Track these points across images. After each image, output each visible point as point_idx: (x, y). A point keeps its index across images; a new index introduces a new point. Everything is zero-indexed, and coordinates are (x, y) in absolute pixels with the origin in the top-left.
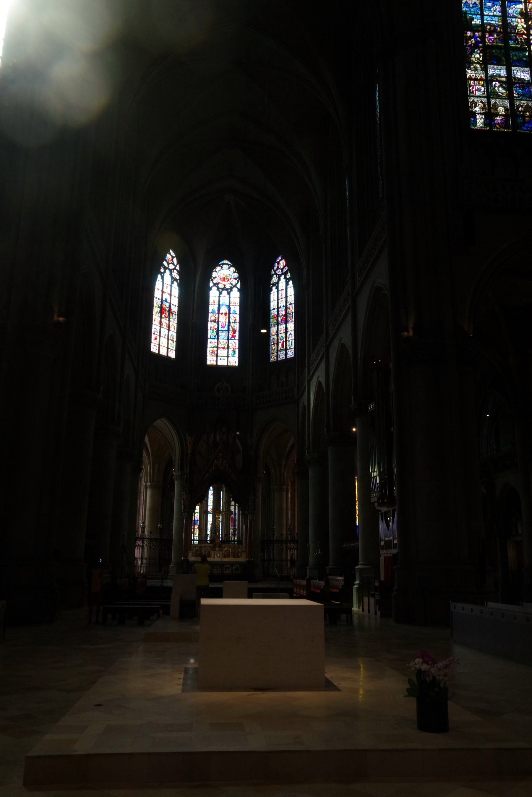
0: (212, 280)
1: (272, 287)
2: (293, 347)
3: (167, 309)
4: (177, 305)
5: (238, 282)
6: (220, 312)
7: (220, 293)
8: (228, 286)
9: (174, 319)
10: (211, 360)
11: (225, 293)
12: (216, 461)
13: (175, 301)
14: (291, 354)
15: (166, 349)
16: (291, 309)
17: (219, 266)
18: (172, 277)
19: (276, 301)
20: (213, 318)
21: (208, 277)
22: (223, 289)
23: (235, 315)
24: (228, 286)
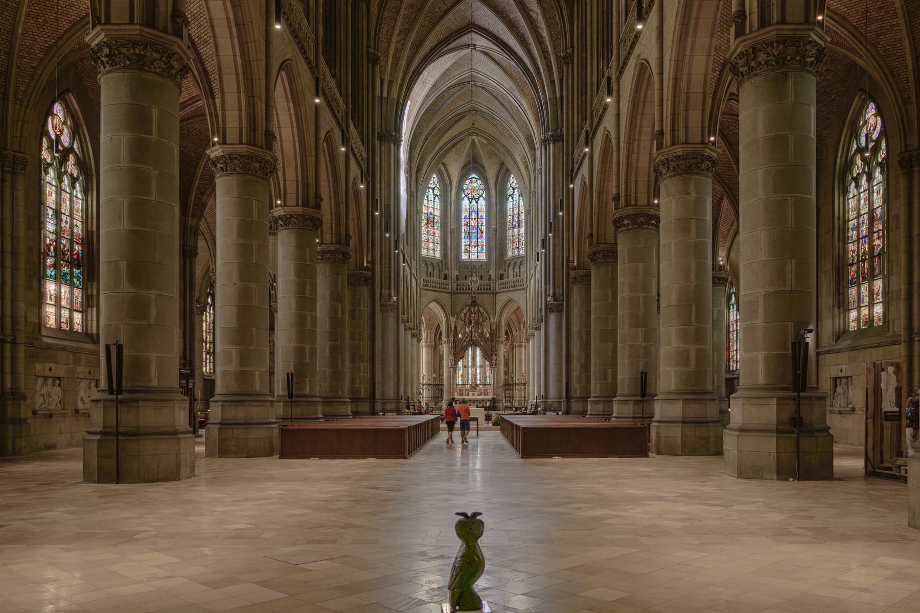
9: (437, 226)
10: (464, 257)
11: (474, 202)
13: (437, 213)
14: (522, 252)
16: (523, 217)
21: (460, 189)
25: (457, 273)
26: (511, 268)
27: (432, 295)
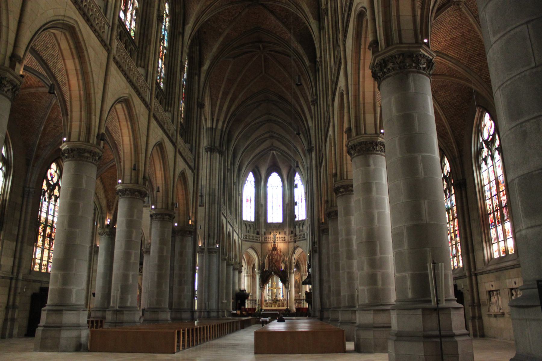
25: (264, 230)
27: (249, 244)
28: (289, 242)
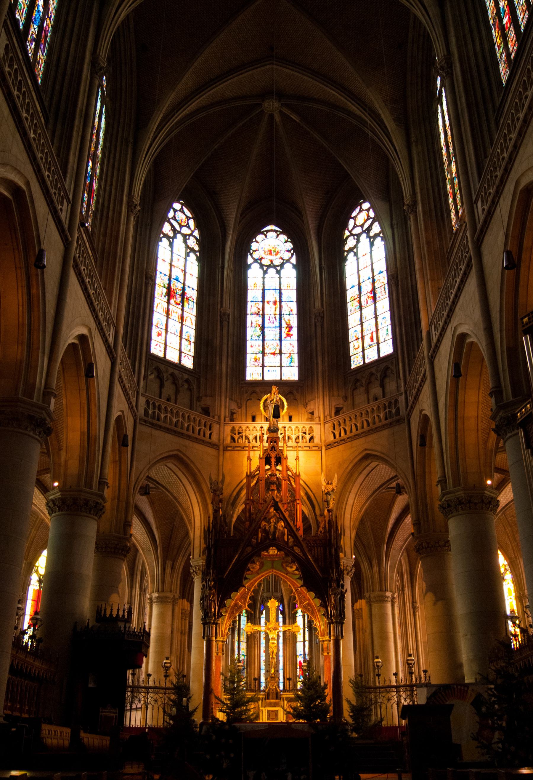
0: (251, 255)
1: (347, 255)
2: (390, 336)
3: (180, 292)
4: (196, 288)
5: (292, 255)
6: (266, 300)
7: (265, 272)
8: (277, 262)
10: (252, 373)
11: (272, 271)
12: (264, 523)
13: (193, 282)
14: (387, 349)
15: (178, 352)
16: (382, 279)
17: (262, 233)
18: (187, 247)
19: (357, 274)
20: (255, 310)
22: (269, 267)
23: (290, 304)
24: (277, 262)
26: (362, 389)
28: (329, 446)
